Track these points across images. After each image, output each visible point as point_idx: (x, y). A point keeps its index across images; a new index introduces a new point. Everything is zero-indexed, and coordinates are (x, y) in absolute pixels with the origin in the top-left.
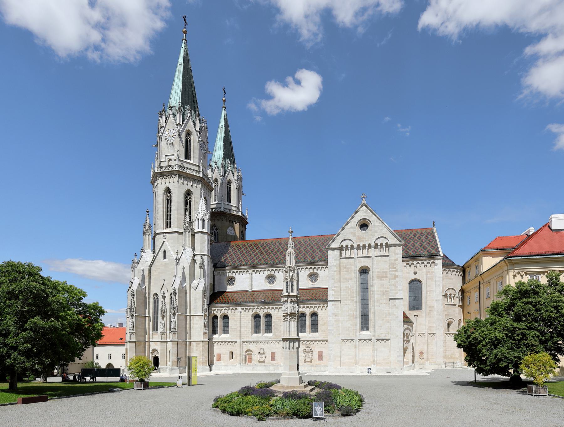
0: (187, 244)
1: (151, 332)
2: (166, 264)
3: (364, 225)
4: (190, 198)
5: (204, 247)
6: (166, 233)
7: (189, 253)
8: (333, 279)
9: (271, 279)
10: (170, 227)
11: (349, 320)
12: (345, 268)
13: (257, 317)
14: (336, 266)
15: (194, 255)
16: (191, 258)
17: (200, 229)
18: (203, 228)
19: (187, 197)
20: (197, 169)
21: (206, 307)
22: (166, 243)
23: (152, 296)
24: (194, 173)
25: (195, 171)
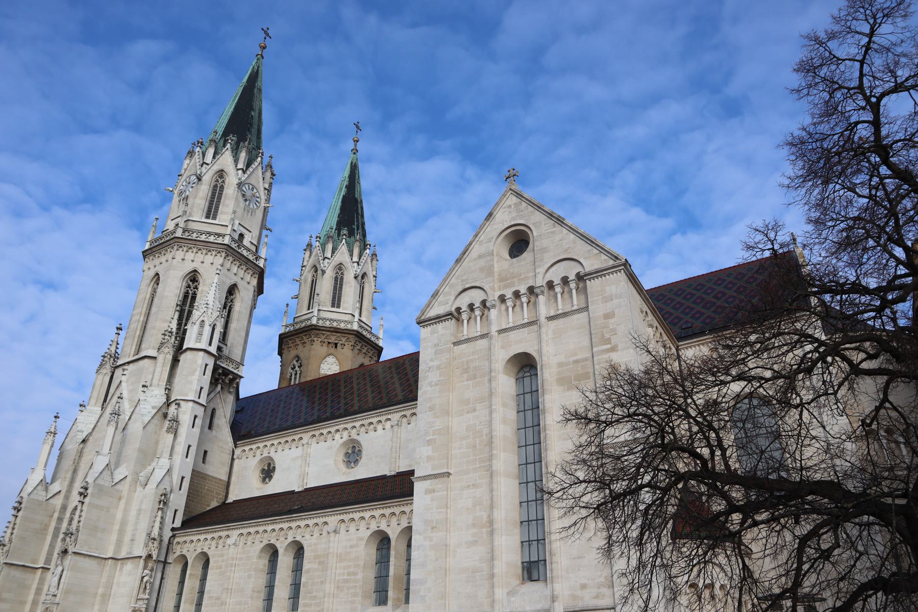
0: (155, 382)
3: (519, 242)
4: (196, 288)
6: (129, 363)
8: (431, 408)
9: (353, 454)
11: (475, 543)
12: (466, 371)
13: (273, 553)
14: (439, 368)
15: (168, 404)
18: (199, 339)
19: (189, 286)
22: (123, 384)
24: (212, 239)
25: (216, 234)
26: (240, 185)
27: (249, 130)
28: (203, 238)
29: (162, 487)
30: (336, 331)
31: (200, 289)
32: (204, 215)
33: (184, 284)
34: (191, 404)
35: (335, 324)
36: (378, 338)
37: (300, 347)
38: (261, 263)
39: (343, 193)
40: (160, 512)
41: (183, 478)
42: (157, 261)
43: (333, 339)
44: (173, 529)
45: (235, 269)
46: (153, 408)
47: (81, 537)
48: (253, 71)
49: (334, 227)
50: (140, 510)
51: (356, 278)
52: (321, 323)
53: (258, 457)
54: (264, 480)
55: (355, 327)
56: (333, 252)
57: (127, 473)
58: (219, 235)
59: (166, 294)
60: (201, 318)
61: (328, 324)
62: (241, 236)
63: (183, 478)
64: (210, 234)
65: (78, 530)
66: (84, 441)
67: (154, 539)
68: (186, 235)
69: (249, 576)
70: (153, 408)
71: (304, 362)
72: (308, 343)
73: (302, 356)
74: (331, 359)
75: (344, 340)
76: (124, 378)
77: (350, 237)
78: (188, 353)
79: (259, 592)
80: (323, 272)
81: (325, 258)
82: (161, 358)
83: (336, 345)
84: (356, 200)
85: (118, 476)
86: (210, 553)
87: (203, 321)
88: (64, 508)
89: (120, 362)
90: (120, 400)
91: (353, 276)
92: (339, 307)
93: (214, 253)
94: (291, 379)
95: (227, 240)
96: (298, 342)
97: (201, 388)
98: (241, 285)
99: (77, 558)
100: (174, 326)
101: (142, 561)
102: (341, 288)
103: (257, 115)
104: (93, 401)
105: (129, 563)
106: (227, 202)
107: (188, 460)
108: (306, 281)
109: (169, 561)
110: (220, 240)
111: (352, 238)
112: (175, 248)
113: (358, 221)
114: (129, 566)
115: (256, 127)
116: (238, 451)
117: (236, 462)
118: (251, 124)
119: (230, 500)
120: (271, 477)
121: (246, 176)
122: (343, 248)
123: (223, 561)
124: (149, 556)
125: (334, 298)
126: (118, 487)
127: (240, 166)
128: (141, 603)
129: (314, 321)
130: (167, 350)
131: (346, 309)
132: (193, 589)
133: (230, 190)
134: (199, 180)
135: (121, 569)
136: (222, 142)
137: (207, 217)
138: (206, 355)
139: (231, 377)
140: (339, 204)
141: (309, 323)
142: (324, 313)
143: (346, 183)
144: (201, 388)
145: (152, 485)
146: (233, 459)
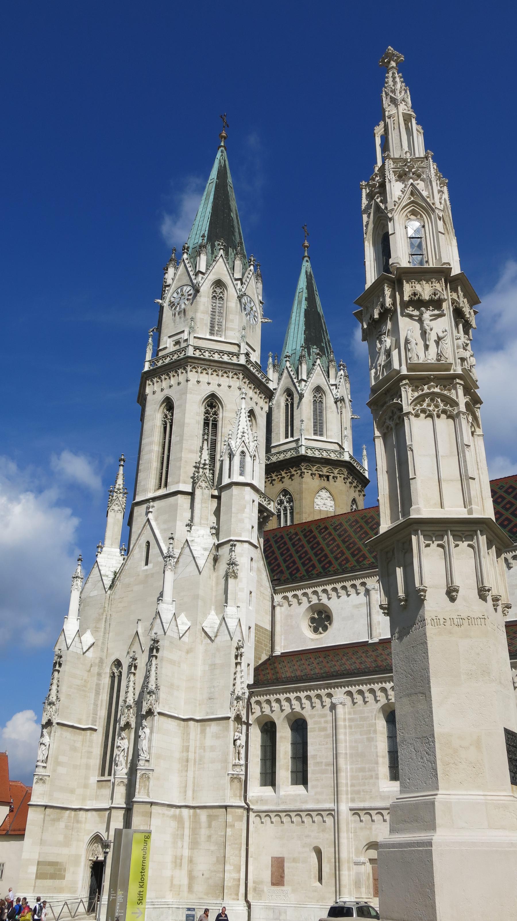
1: (94, 777)
2: (147, 576)
4: (215, 413)
5: (242, 521)
6: (154, 499)
7: (202, 540)
10: (166, 485)
15: (218, 547)
16: (207, 553)
17: (237, 478)
18: (242, 474)
19: (207, 412)
20: (234, 349)
21: (241, 689)
23: (107, 671)
24: (226, 358)
25: (229, 353)
26: (240, 298)
27: (235, 236)
28: (216, 357)
29: (236, 639)
30: (327, 462)
31: (220, 415)
32: (208, 331)
33: (203, 410)
34: (246, 545)
35: (325, 455)
36: (364, 470)
37: (286, 480)
38: (271, 386)
39: (304, 305)
40: (238, 666)
41: (250, 628)
42: (165, 384)
43: (325, 471)
44: (249, 686)
45: (251, 393)
46: (205, 549)
47: (162, 694)
48: (220, 166)
49: (304, 345)
50: (213, 667)
51: (336, 403)
52: (310, 454)
53: (305, 604)
54: (316, 630)
55: (346, 457)
56: (309, 373)
57: (189, 624)
58: (233, 354)
59: (187, 421)
60: (241, 449)
61: (317, 454)
62: (247, 355)
63: (250, 628)
64: (221, 352)
65: (157, 687)
66: (111, 587)
67: (238, 698)
68: (198, 354)
69: (370, 740)
70: (205, 549)
71: (295, 496)
72: (296, 477)
73: (290, 489)
74: (324, 494)
75: (336, 471)
76: (150, 516)
77: (321, 357)
78: (234, 488)
79: (383, 757)
80: (301, 396)
81: (300, 382)
82: (198, 492)
83: (328, 477)
84: (319, 314)
85: (183, 628)
86: (304, 712)
87: (243, 452)
88: (101, 661)
89: (138, 499)
90: (171, 541)
91: (333, 400)
92: (321, 435)
93: (231, 375)
94: (279, 516)
95: (242, 360)
96: (284, 475)
97: (253, 527)
98: (257, 410)
99: (162, 718)
100: (206, 456)
101: (231, 722)
102: (321, 412)
103: (235, 217)
104: (107, 542)
105: (213, 723)
106: (231, 317)
107: (250, 608)
108: (279, 406)
109: (250, 722)
110: (235, 360)
111: (324, 358)
112: (189, 368)
113: (325, 339)
114: (214, 727)
115: (237, 230)
116: (278, 598)
117: (278, 609)
118: (233, 228)
119: (277, 653)
120: (325, 629)
121: (245, 286)
122: (318, 370)
123: (326, 722)
124: (238, 719)
125: (315, 426)
126: (185, 639)
127: (238, 275)
128: (238, 769)
129: (303, 451)
130: (204, 485)
131: (331, 437)
132: (286, 753)
133: (232, 303)
134: (197, 291)
135: (203, 732)
136: (209, 247)
137: (211, 334)
138: (252, 491)
139: (265, 514)
140: (302, 319)
141: (295, 455)
142: (308, 443)
143: (305, 295)
144: (253, 527)
145: (224, 637)
146: (273, 607)
